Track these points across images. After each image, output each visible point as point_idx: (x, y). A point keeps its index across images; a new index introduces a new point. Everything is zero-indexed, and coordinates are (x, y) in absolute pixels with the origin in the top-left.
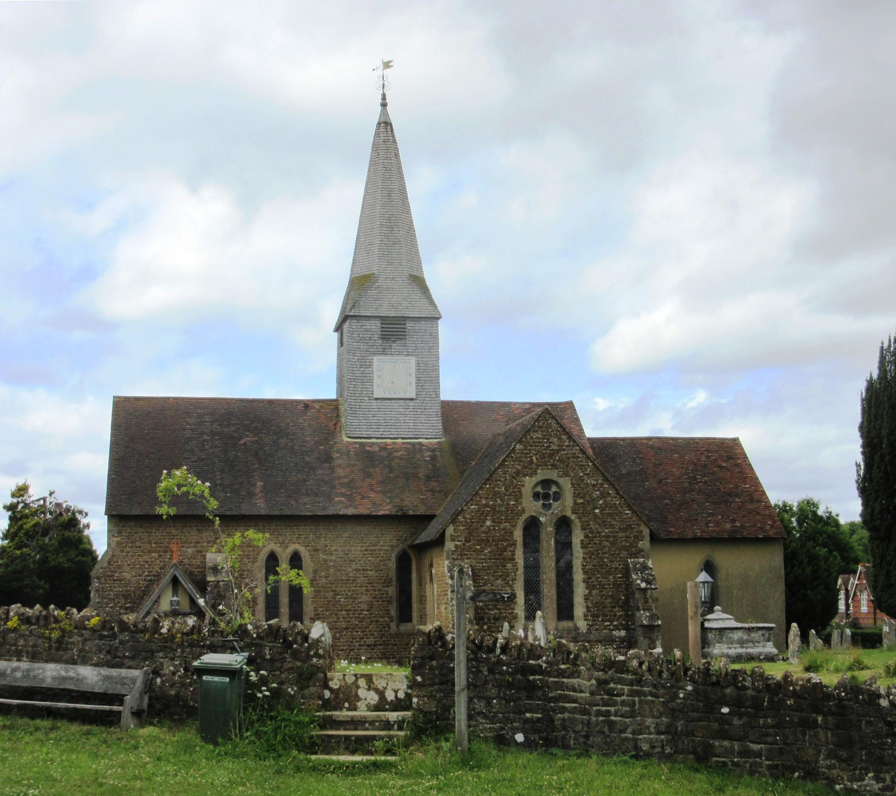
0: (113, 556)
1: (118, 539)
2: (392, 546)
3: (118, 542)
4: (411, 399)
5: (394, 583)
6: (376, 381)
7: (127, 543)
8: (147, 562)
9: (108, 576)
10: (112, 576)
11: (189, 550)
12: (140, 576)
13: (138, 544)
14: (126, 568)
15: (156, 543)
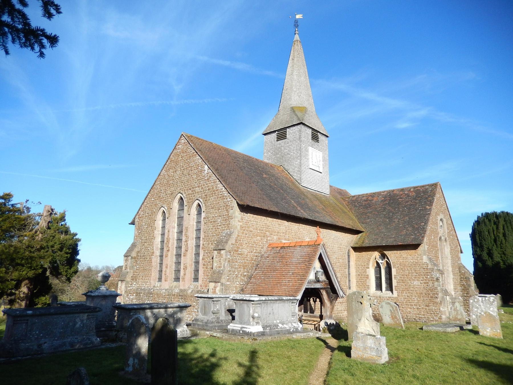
0: (238, 236)
1: (241, 224)
2: (346, 246)
3: (241, 226)
4: (321, 173)
5: (347, 267)
6: (310, 160)
7: (245, 227)
8: (255, 242)
9: (235, 251)
10: (237, 251)
11: (275, 237)
12: (252, 252)
13: (251, 229)
14: (245, 246)
15: (260, 230)
